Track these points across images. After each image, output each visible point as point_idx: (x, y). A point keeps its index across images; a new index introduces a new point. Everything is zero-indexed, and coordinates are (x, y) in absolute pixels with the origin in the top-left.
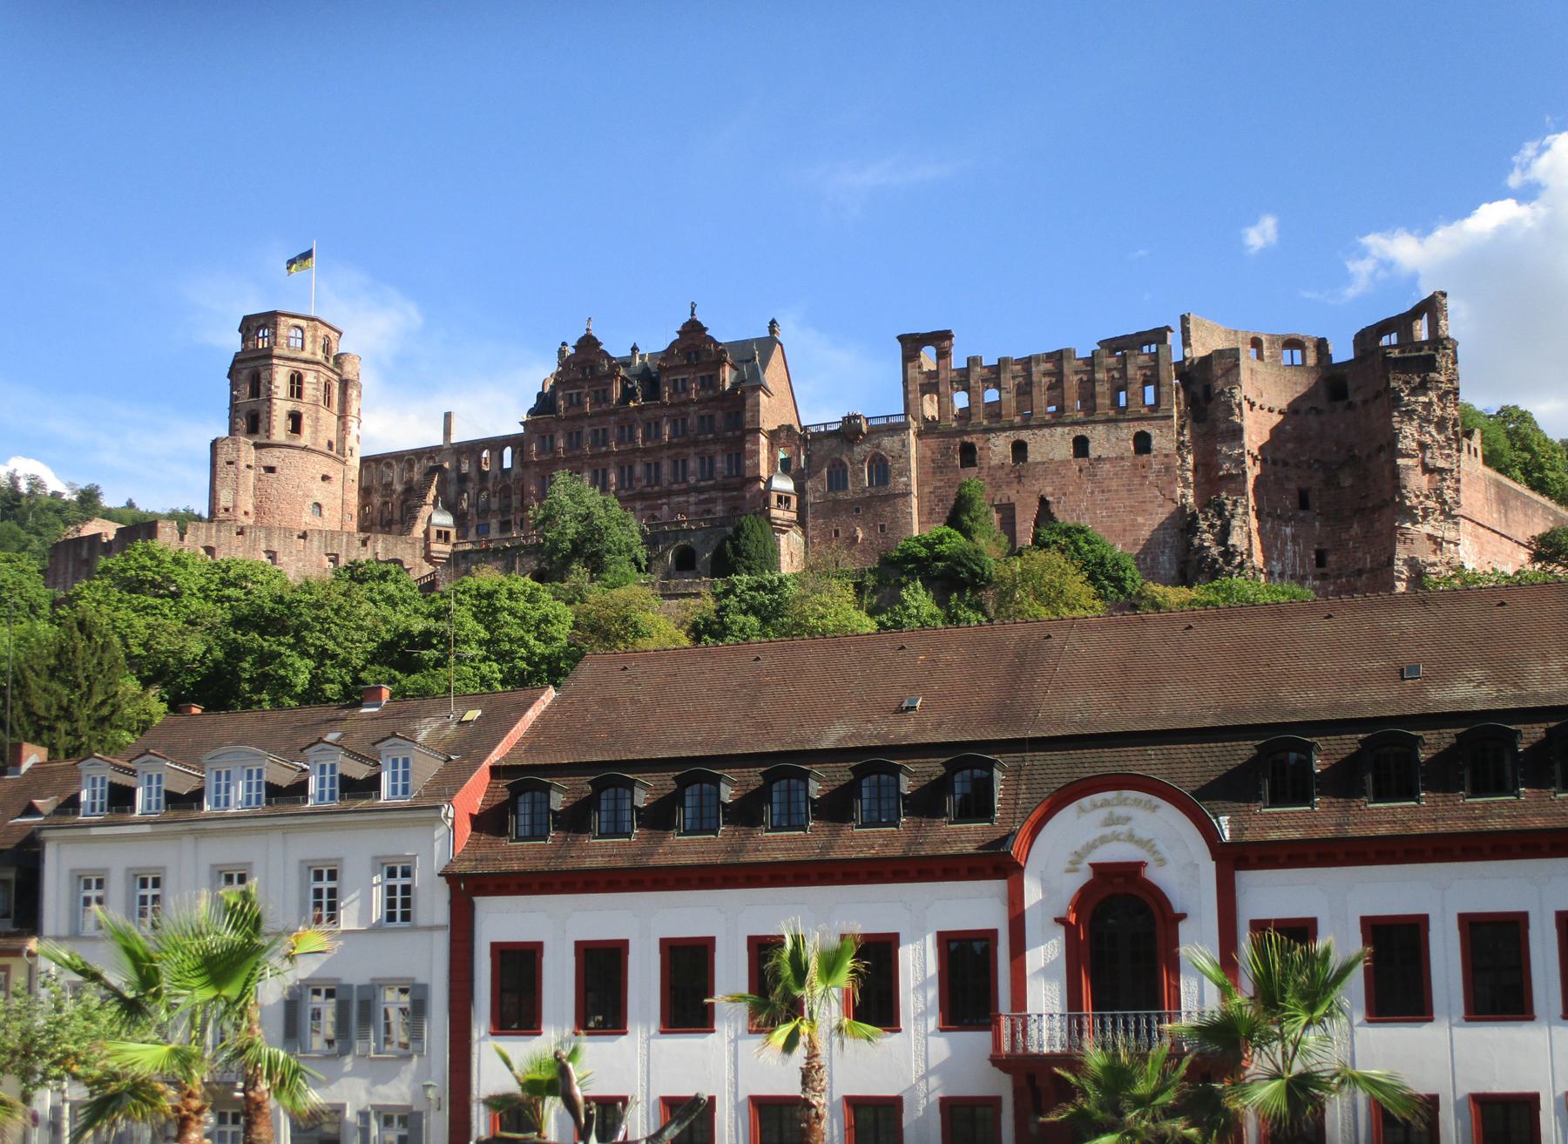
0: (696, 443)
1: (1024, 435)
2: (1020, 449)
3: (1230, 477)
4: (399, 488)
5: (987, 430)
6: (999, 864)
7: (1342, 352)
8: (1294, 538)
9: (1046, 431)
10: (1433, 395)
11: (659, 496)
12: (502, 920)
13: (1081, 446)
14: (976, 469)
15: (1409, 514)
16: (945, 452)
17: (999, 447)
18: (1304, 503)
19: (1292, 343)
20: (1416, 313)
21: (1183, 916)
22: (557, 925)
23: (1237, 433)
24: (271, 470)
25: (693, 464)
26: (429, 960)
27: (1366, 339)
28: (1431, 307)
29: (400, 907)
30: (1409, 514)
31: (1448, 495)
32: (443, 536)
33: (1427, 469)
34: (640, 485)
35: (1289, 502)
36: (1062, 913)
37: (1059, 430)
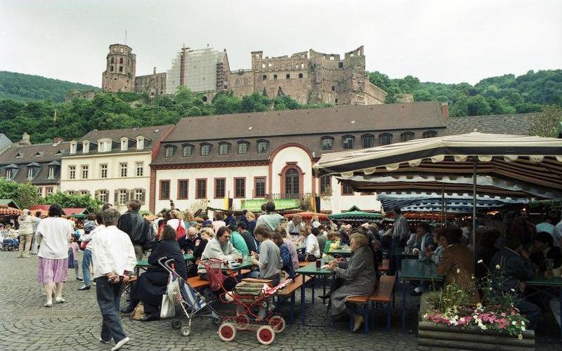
2: (276, 76)
6: (267, 162)
7: (342, 58)
12: (162, 175)
13: (288, 76)
14: (265, 81)
15: (354, 91)
16: (260, 77)
17: (271, 76)
18: (333, 89)
19: (332, 55)
20: (358, 50)
21: (304, 174)
22: (174, 176)
23: (320, 74)
26: (144, 183)
27: (347, 55)
28: (361, 49)
29: (140, 172)
30: (354, 91)
32: (153, 94)
33: (359, 83)
35: (330, 89)
36: (280, 173)
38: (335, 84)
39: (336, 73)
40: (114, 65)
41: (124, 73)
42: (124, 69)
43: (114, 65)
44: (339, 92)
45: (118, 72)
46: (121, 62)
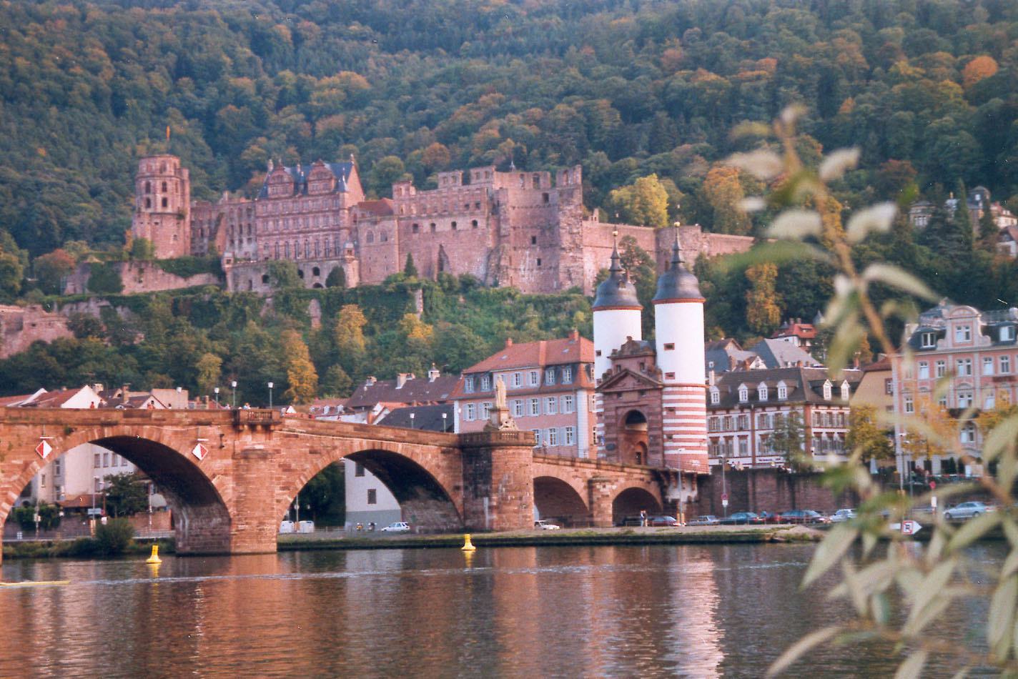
0: (322, 212)
2: (433, 225)
3: (505, 236)
5: (421, 218)
8: (530, 255)
10: (572, 207)
11: (309, 232)
13: (454, 224)
14: (417, 235)
15: (563, 249)
16: (407, 226)
17: (426, 225)
23: (506, 220)
24: (157, 223)
25: (321, 220)
31: (578, 242)
32: (228, 262)
33: (571, 233)
34: (301, 228)
35: (528, 242)
38: (537, 233)
39: (538, 212)
40: (151, 196)
41: (169, 210)
43: (151, 196)
44: (543, 248)
45: (159, 209)
46: (164, 190)
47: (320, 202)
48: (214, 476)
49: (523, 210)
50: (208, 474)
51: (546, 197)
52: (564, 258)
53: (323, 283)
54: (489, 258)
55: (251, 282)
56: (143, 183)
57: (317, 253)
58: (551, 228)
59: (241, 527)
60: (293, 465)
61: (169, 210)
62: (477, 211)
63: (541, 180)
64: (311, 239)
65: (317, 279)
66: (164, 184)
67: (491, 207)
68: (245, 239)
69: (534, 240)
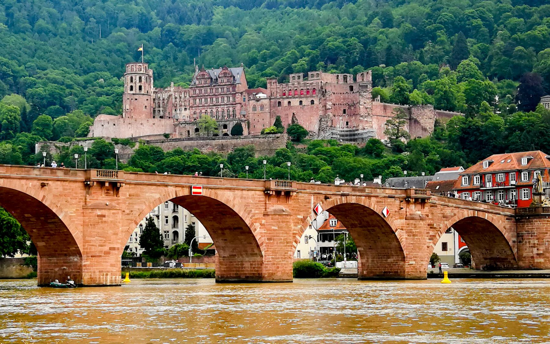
1: (290, 100)
2: (289, 102)
4: (161, 99)
5: (283, 99)
9: (294, 99)
13: (301, 102)
14: (280, 107)
15: (362, 116)
16: (275, 103)
17: (285, 102)
24: (136, 99)
25: (226, 99)
30: (362, 116)
34: (214, 103)
35: (342, 112)
37: (297, 99)
41: (143, 92)
42: (143, 87)
47: (225, 89)
48: (396, 230)
49: (340, 95)
50: (394, 229)
51: (351, 88)
52: (361, 121)
53: (229, 133)
54: (320, 121)
55: (189, 132)
56: (129, 78)
57: (223, 116)
58: (354, 105)
59: (411, 263)
60: (435, 225)
61: (143, 92)
62: (314, 95)
63: (348, 79)
64: (220, 109)
65: (225, 131)
66: (140, 78)
67: (322, 92)
68: (183, 109)
69: (344, 111)
